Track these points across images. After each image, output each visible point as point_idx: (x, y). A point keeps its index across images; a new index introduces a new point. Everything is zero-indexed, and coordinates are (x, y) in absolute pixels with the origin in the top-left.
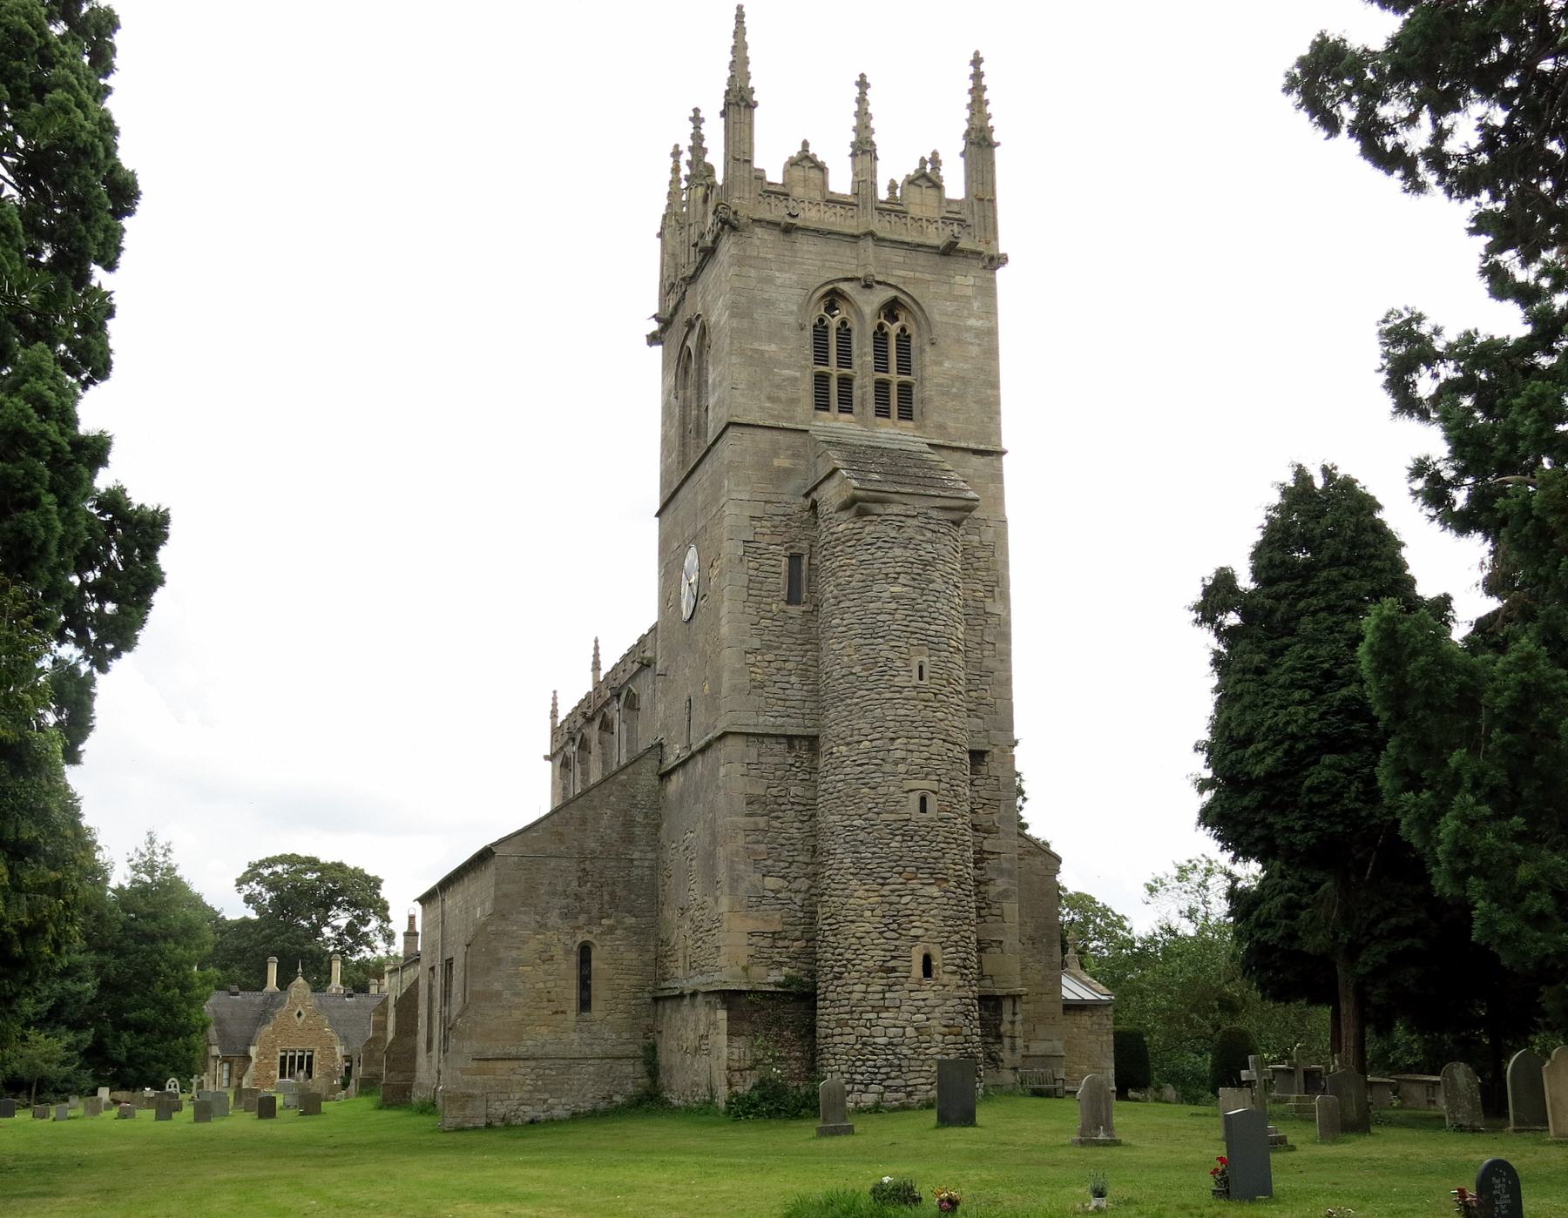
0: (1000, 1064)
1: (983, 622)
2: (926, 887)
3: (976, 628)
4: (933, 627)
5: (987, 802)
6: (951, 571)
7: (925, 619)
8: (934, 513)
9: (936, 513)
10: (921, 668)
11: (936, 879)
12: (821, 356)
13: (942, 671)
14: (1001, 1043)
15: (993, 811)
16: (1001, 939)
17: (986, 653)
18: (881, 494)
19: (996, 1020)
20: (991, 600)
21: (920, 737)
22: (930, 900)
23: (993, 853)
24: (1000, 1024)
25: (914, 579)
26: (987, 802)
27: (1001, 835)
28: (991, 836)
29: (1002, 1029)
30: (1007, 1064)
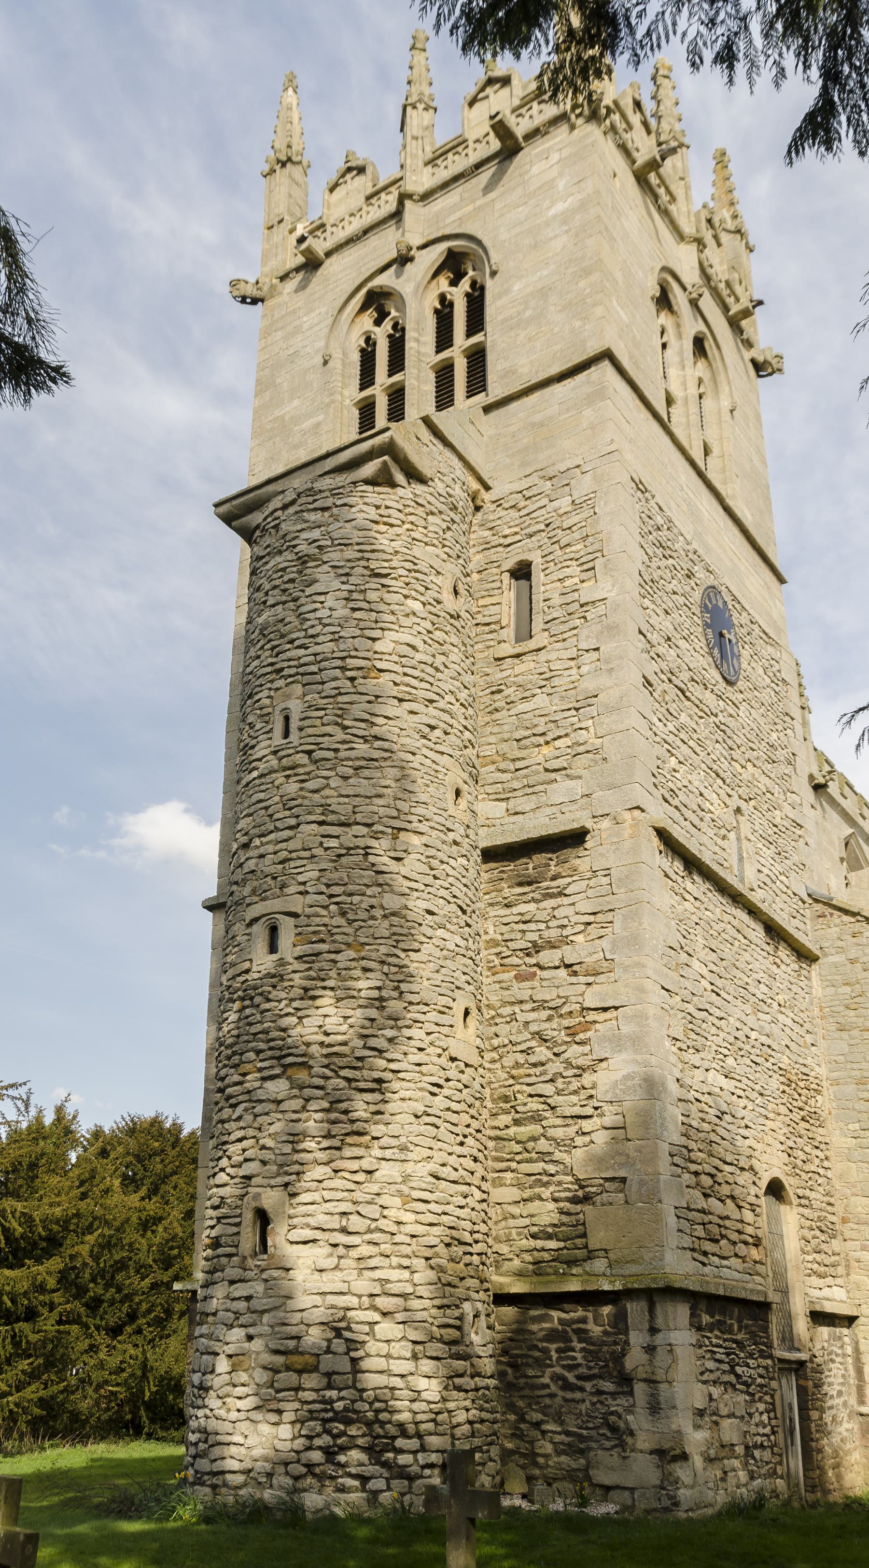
0: (629, 1440)
1: (578, 622)
2: (269, 1085)
3: (565, 636)
4: (309, 651)
5: (591, 918)
6: (360, 555)
7: (297, 643)
8: (327, 482)
9: (331, 481)
10: (287, 719)
11: (285, 1067)
12: (367, 377)
13: (322, 713)
14: (631, 1393)
15: (602, 932)
16: (622, 1173)
17: (585, 669)
18: (251, 495)
19: (615, 1343)
20: (593, 581)
21: (277, 829)
22: (272, 1106)
23: (605, 1009)
24: (624, 1355)
25: (284, 591)
26: (591, 918)
27: (618, 973)
28: (601, 978)
29: (629, 1363)
30: (644, 1441)
